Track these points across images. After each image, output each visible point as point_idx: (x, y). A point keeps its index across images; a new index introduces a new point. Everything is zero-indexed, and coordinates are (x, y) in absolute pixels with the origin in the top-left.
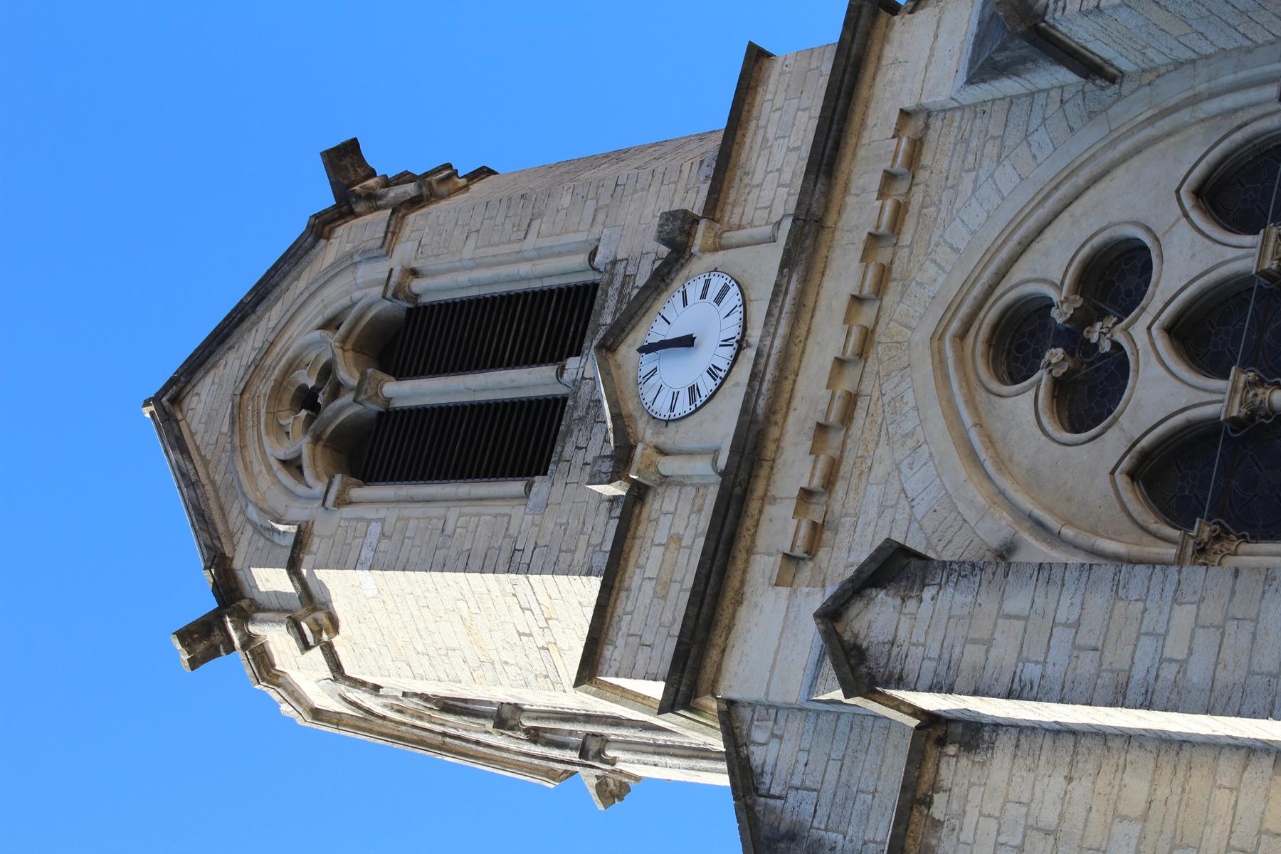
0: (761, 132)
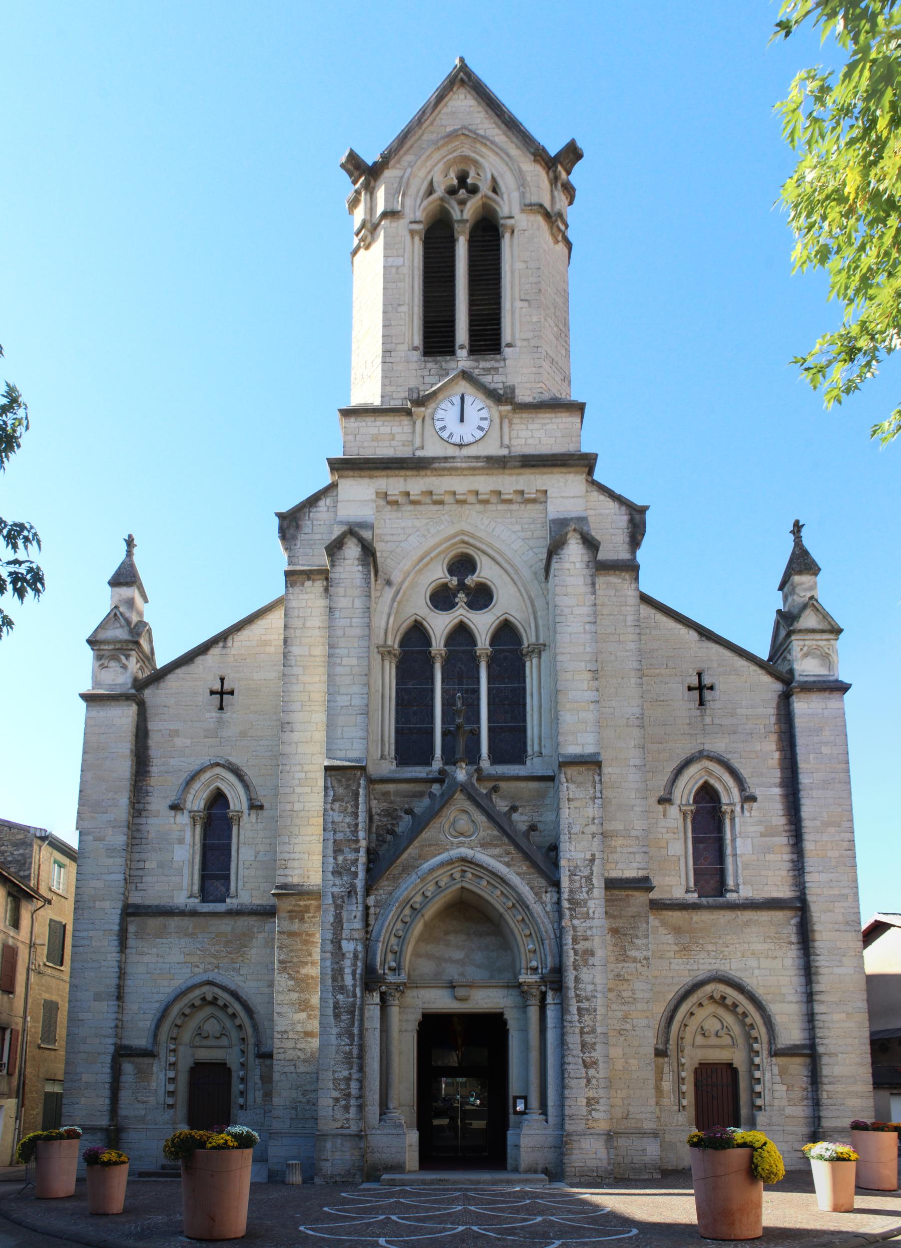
0: (547, 421)
